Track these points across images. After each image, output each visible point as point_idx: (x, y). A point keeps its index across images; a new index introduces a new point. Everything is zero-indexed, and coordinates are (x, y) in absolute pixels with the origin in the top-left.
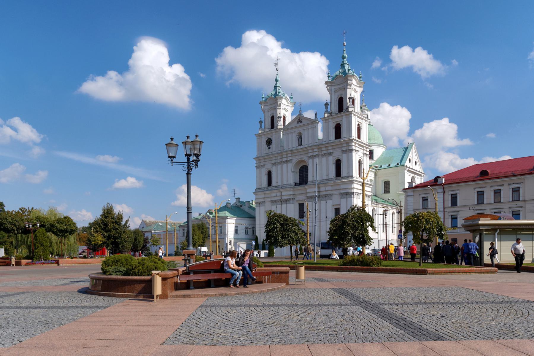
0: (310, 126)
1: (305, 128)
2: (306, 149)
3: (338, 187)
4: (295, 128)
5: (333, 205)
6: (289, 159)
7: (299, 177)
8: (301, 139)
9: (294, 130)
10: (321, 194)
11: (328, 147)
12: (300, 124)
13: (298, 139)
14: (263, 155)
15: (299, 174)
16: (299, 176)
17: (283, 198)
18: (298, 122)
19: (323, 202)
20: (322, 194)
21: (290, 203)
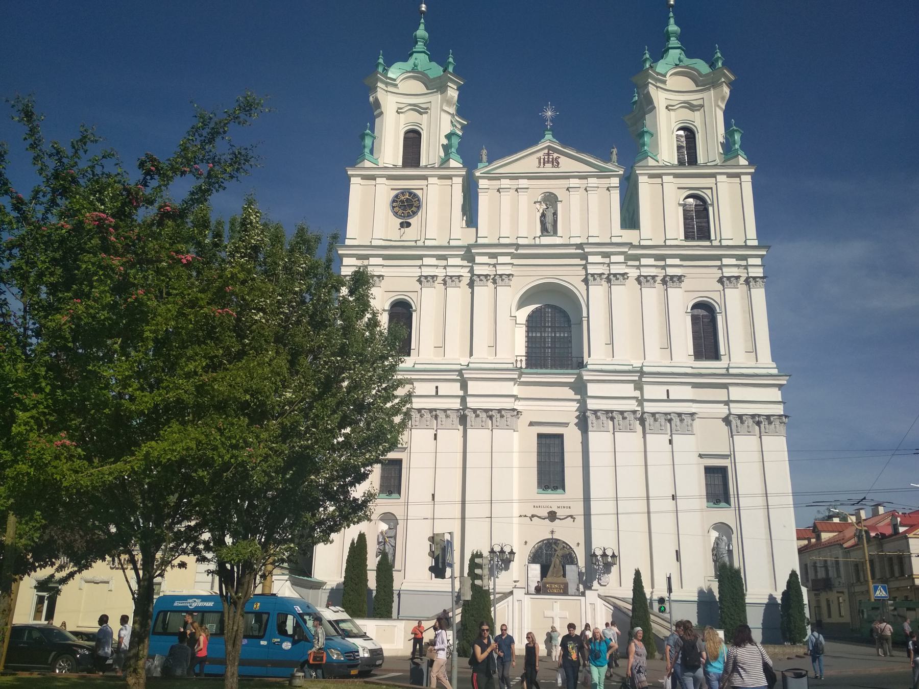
0: (592, 181)
1: (574, 182)
2: (581, 252)
3: (721, 394)
4: (529, 178)
5: (701, 456)
6: (501, 270)
7: (527, 342)
8: (555, 214)
9: (523, 183)
10: (646, 410)
11: (662, 258)
12: (549, 169)
13: (543, 215)
14: (375, 243)
15: (527, 332)
16: (527, 337)
17: (472, 403)
18: (543, 162)
19: (657, 441)
20: (649, 407)
21: (508, 427)
